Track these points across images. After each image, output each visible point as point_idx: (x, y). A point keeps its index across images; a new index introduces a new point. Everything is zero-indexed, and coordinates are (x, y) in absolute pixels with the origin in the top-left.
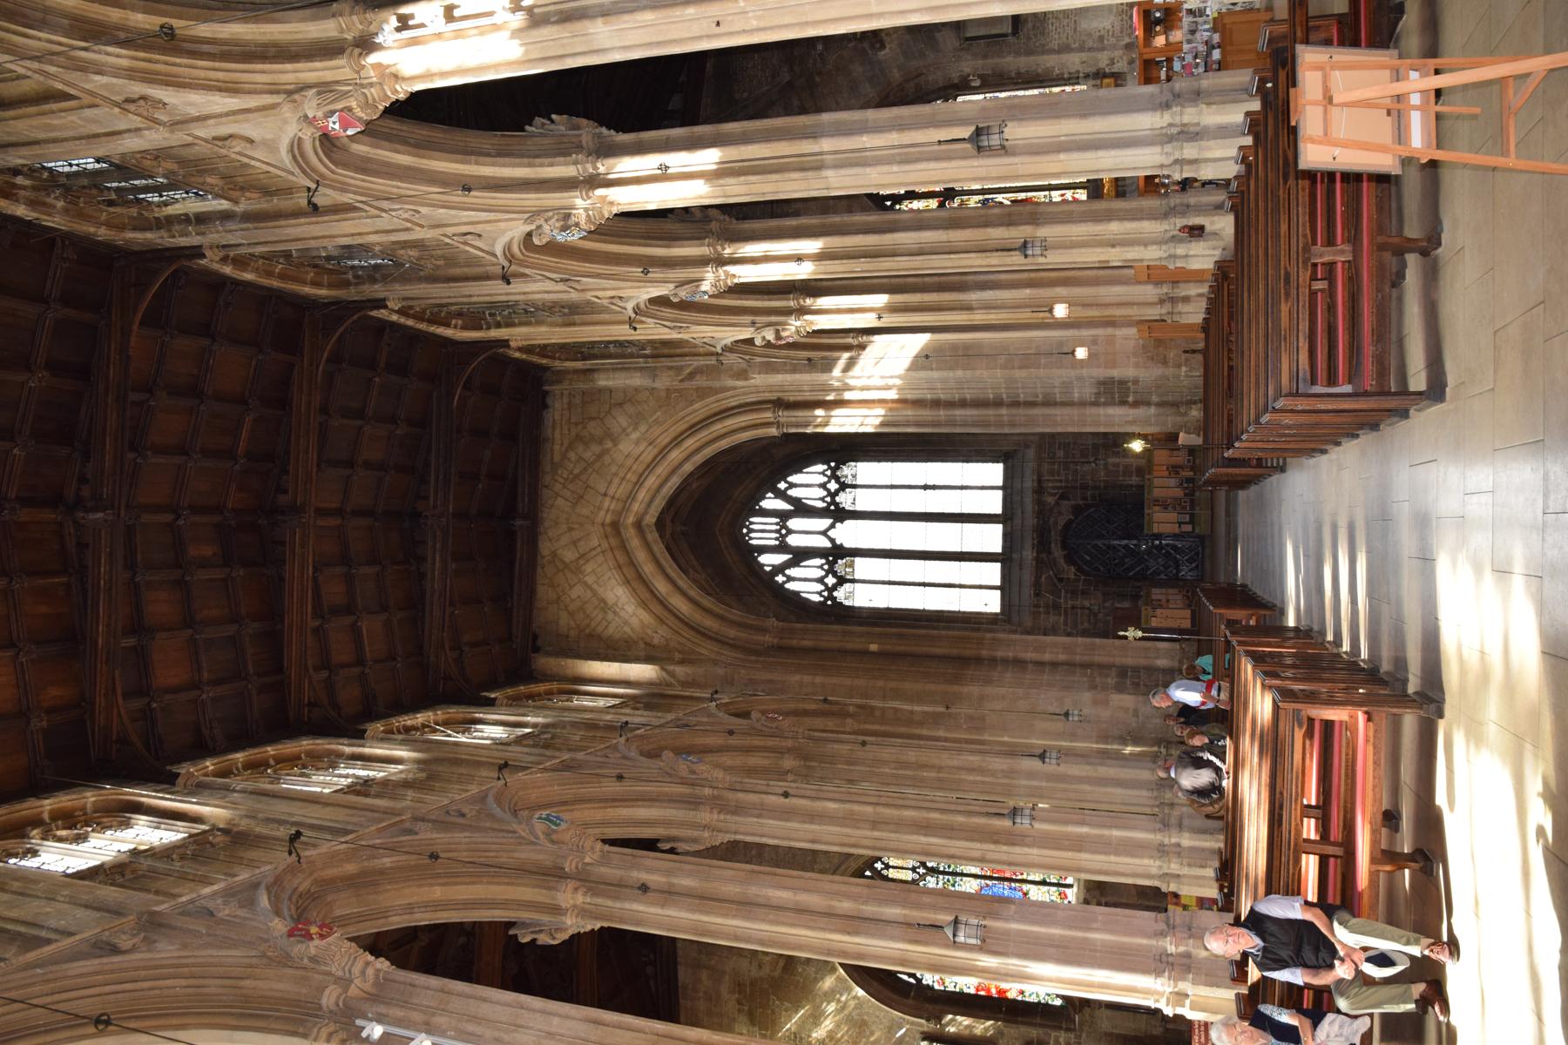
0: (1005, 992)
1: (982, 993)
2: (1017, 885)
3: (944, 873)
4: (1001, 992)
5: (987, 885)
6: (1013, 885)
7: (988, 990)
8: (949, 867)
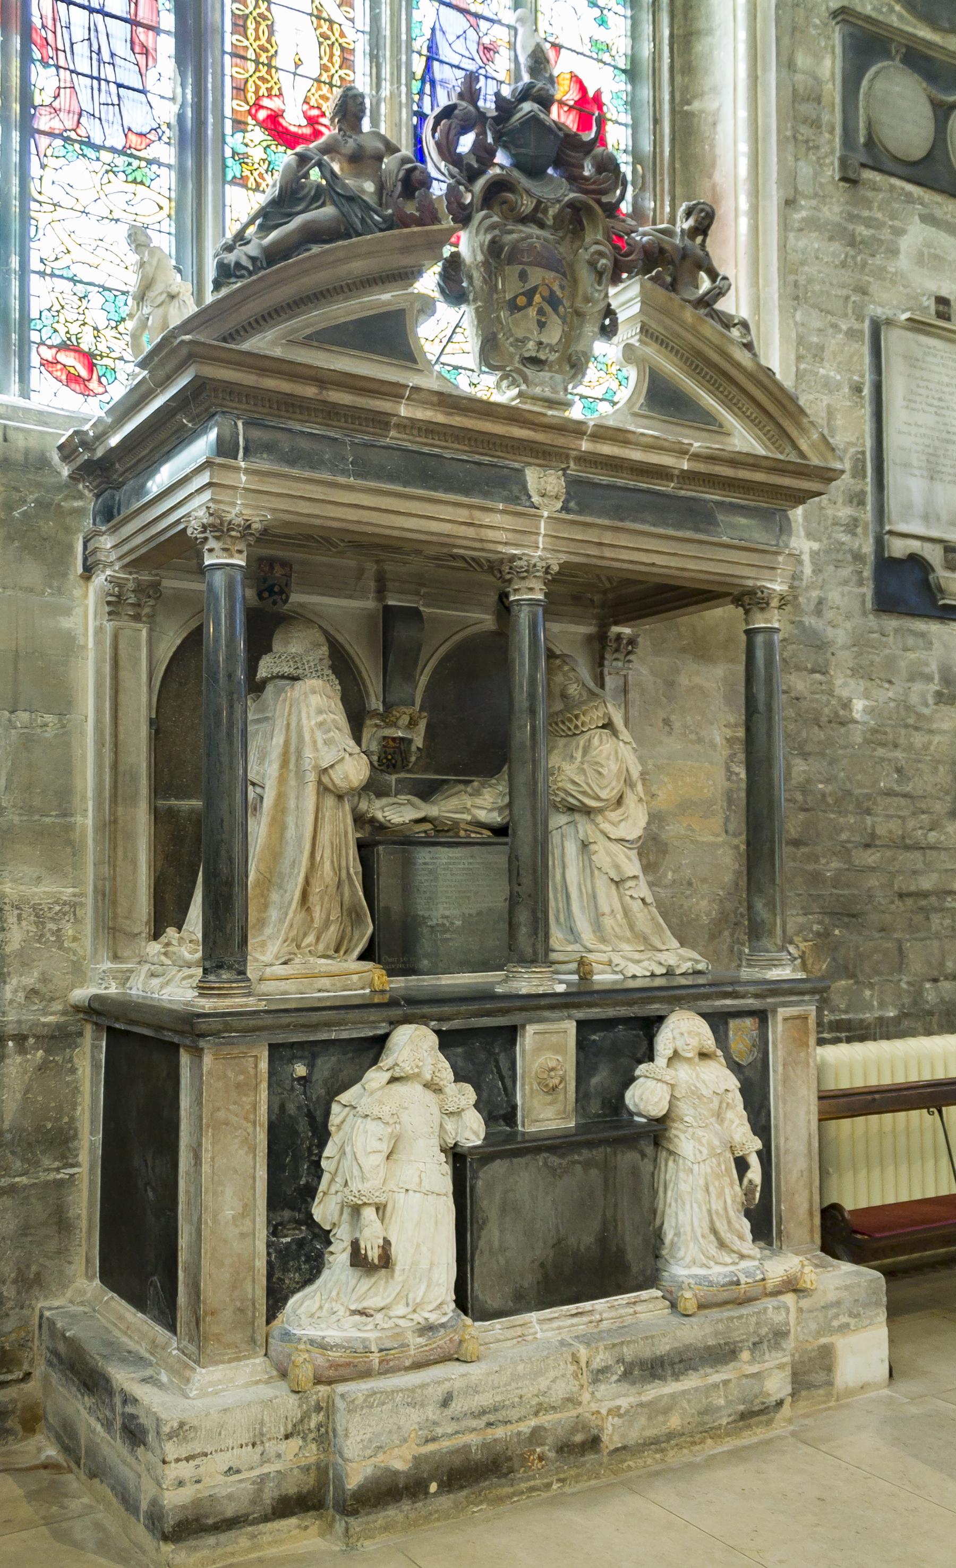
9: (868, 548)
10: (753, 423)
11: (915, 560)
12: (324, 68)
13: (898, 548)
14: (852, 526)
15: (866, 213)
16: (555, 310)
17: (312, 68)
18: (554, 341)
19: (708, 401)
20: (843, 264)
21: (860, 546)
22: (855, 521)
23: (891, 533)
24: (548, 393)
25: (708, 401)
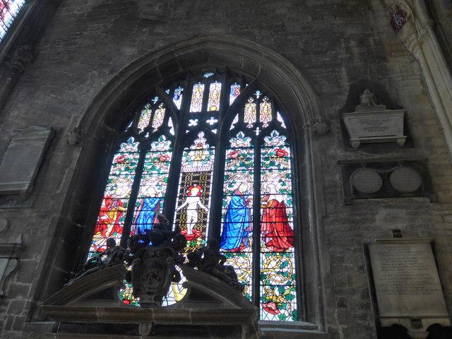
0: (102, 231)
1: (104, 203)
2: (251, 240)
3: (258, 155)
4: (103, 225)
5: (247, 203)
6: (251, 234)
7: (106, 211)
8: (267, 159)
9: (373, 324)
10: (228, 298)
11: (395, 326)
12: (199, 220)
13: (386, 323)
14: (364, 317)
15: (359, 212)
16: (155, 278)
17: (195, 220)
18: (156, 286)
19: (214, 293)
20: (350, 229)
21: (369, 324)
22: (365, 315)
23: (382, 317)
24: (149, 301)
25: (214, 293)
